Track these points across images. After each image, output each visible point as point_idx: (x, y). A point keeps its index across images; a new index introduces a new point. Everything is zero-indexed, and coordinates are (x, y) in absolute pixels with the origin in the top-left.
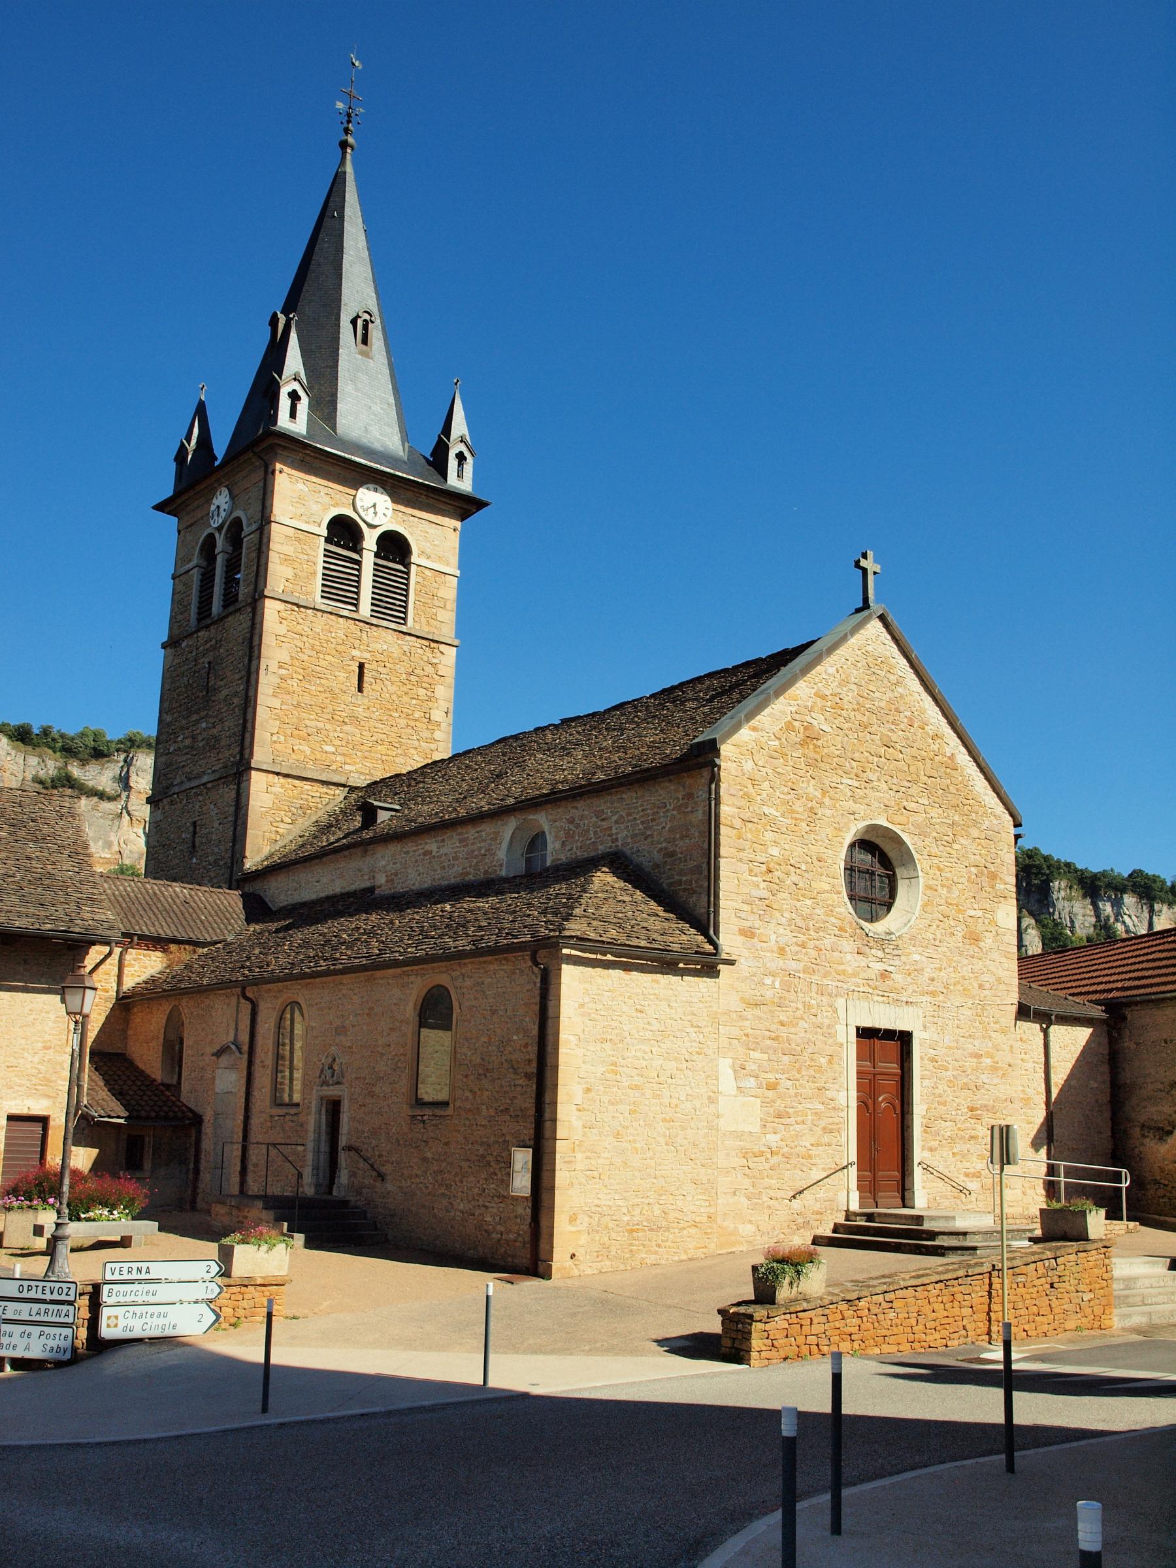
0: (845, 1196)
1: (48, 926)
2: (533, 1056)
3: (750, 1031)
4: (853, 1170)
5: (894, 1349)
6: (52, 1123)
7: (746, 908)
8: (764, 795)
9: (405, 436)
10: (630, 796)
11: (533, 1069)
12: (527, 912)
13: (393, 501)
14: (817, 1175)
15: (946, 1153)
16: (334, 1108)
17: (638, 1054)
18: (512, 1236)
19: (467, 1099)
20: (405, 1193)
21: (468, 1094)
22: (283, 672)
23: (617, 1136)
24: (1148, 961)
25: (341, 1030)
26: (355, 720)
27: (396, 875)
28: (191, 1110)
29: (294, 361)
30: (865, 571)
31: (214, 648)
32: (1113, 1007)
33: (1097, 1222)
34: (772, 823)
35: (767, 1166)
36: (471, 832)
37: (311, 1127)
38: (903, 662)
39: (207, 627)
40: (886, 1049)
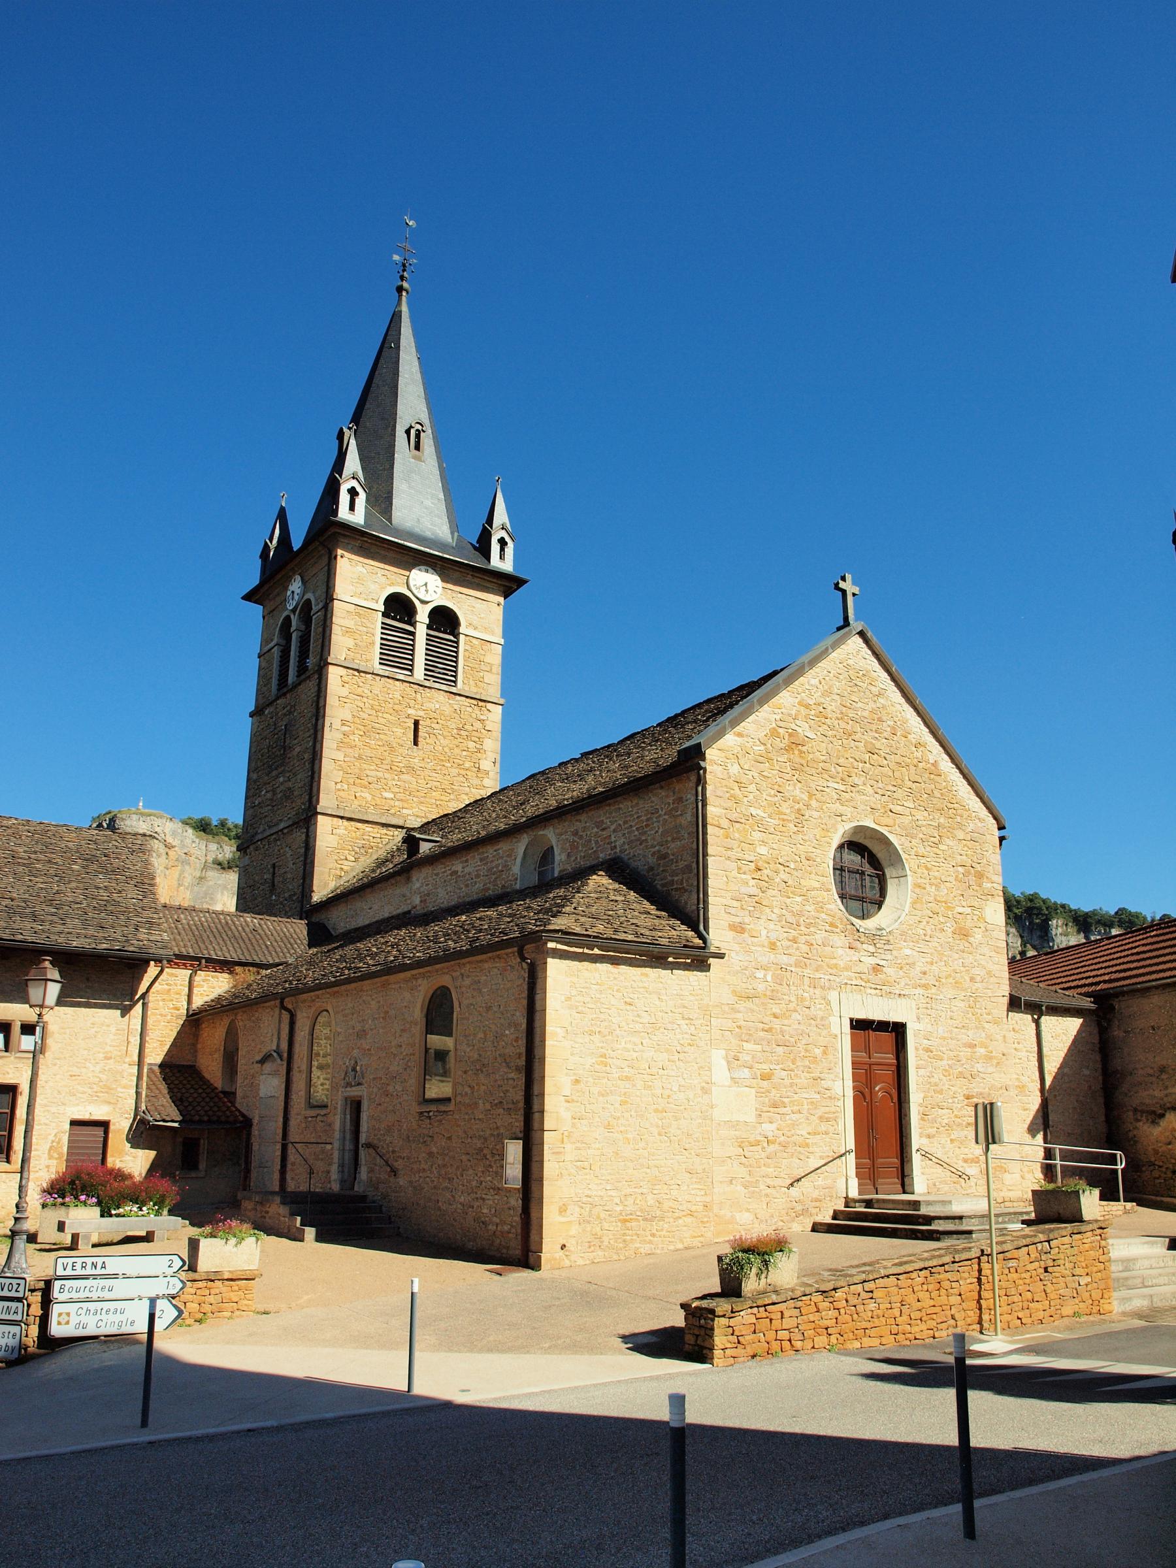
0: (843, 1183)
1: (105, 946)
2: (523, 1050)
3: (742, 1023)
4: (851, 1159)
5: (875, 1342)
6: (112, 1127)
7: (735, 904)
8: (751, 797)
9: (454, 527)
10: (627, 806)
11: (522, 1062)
12: (527, 913)
13: (443, 580)
14: (814, 1163)
15: (945, 1140)
16: (356, 1106)
17: (629, 1046)
18: (506, 1228)
19: (466, 1094)
20: (415, 1188)
21: (467, 1090)
22: (346, 728)
23: (608, 1126)
24: (1132, 954)
25: (362, 1034)
26: (411, 769)
27: (428, 895)
28: (243, 1115)
29: (353, 463)
30: (844, 592)
31: (290, 712)
32: (1098, 997)
33: (1091, 1203)
34: (760, 825)
35: (763, 1155)
36: (489, 851)
37: (337, 1125)
38: (884, 675)
39: (285, 694)
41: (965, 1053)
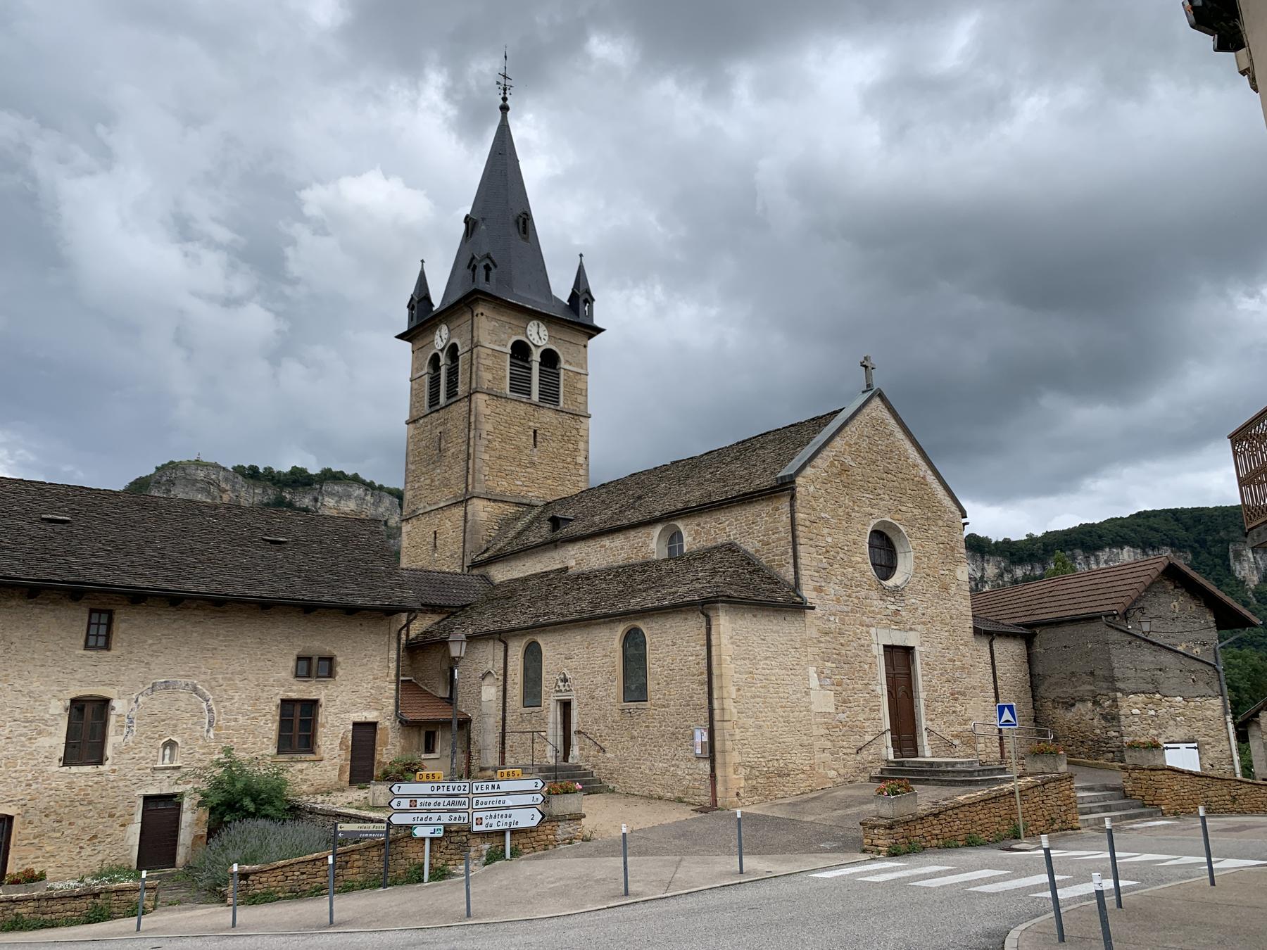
4: (889, 735)
11: (705, 677)
14: (868, 738)
40: (900, 659)
41: (949, 666)
